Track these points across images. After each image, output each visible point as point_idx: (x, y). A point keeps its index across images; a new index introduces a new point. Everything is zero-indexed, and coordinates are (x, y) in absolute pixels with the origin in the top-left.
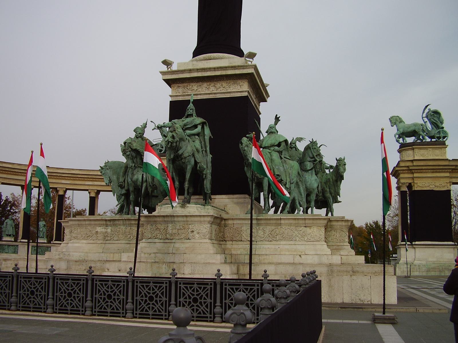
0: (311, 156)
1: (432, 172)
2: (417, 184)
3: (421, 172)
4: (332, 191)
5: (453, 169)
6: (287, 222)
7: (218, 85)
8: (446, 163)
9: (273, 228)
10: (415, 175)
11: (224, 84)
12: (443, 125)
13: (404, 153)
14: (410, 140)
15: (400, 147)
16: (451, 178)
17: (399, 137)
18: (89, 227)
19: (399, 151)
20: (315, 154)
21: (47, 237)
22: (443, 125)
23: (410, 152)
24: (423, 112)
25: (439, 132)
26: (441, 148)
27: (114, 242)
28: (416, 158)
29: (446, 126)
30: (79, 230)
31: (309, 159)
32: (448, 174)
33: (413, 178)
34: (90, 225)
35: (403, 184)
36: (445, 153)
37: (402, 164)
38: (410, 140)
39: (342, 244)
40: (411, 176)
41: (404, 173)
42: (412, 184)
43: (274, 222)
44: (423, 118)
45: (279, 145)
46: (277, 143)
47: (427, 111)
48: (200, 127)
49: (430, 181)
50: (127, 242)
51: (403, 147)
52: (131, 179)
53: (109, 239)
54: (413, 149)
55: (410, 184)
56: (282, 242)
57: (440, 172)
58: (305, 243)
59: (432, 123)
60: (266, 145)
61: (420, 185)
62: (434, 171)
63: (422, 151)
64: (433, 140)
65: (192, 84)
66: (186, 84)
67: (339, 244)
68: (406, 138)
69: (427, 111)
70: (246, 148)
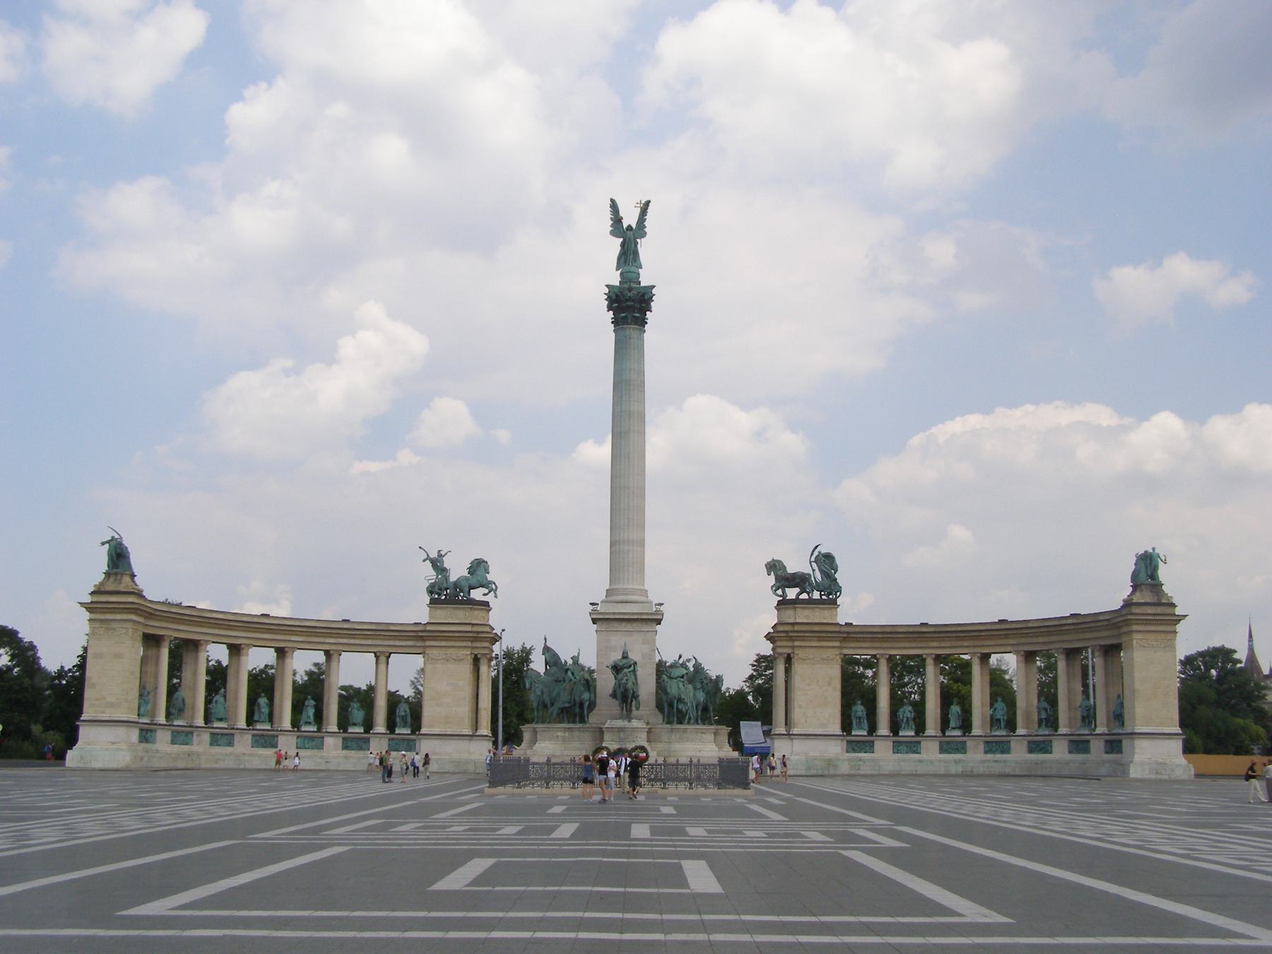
8: (837, 629)
10: (797, 643)
14: (792, 593)
15: (779, 603)
32: (837, 644)
33: (793, 647)
35: (780, 654)
37: (780, 628)
38: (792, 593)
40: (790, 644)
47: (816, 553)
51: (783, 604)
59: (821, 571)
62: (820, 639)
63: (807, 612)
69: (816, 553)
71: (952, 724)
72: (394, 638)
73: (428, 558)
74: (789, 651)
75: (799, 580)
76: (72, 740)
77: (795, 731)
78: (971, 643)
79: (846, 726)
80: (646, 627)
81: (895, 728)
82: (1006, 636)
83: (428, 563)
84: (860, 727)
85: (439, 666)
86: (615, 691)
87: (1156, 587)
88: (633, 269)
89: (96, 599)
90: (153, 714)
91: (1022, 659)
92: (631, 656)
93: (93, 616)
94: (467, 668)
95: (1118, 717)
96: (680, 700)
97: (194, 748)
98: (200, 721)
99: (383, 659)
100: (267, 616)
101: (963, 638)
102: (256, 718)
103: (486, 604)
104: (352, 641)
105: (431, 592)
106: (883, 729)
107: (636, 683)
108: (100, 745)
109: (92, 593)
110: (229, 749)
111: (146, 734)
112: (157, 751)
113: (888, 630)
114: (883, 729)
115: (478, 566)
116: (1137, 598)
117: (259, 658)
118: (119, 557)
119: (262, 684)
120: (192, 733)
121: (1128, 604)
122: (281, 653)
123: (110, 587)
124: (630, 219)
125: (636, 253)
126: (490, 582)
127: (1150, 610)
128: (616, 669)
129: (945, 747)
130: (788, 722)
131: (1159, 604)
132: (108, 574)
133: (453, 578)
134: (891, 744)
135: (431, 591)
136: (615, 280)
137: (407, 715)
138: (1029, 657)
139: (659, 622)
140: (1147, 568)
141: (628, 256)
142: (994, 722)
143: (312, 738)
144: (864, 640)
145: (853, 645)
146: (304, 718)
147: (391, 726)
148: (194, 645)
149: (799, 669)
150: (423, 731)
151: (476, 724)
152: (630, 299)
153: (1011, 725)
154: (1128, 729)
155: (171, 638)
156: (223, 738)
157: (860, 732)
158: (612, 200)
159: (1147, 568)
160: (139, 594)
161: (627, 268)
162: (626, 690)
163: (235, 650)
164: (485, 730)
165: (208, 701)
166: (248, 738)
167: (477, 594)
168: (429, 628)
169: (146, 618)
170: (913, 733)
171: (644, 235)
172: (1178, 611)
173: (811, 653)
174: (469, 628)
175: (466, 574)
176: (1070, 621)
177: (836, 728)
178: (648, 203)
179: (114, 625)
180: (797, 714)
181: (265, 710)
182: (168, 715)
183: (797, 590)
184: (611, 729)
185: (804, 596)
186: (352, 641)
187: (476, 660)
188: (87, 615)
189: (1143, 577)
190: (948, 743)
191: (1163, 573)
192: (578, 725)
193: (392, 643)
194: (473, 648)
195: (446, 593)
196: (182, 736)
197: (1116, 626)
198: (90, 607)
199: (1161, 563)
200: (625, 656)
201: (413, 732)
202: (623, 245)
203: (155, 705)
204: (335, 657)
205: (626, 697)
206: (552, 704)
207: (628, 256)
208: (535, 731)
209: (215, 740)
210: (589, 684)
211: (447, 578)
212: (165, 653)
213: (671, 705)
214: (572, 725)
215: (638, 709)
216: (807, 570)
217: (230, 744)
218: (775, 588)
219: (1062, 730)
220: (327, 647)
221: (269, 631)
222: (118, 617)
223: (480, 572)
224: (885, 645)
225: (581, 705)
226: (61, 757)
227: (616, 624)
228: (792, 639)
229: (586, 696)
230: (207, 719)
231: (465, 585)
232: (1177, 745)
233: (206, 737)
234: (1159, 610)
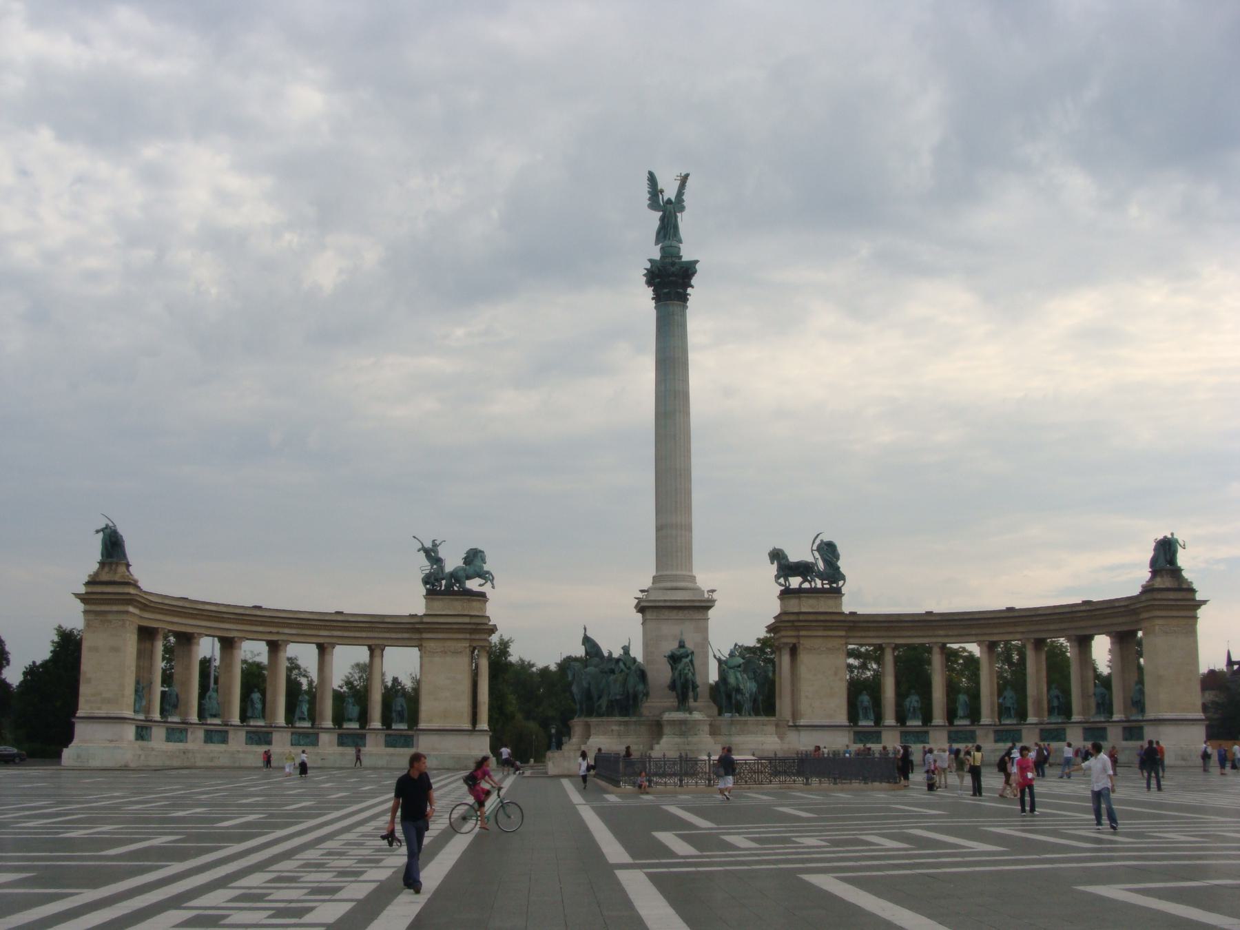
10: (803, 633)
14: (795, 582)
16: (847, 637)
28: (804, 610)
29: (843, 564)
32: (843, 633)
35: (786, 644)
37: (786, 618)
38: (795, 582)
40: (793, 633)
47: (818, 542)
51: (786, 593)
59: (824, 560)
62: (826, 628)
63: (811, 602)
71: (960, 712)
72: (389, 630)
75: (803, 569)
76: (67, 737)
77: (802, 722)
78: (978, 631)
79: (853, 716)
80: (697, 615)
81: (901, 718)
82: (1015, 624)
83: (422, 554)
84: (866, 717)
87: (1176, 572)
88: (675, 243)
89: (90, 590)
90: (147, 710)
91: (985, 649)
92: (687, 645)
93: (88, 608)
95: (1138, 704)
96: (738, 690)
97: (190, 746)
98: (194, 718)
100: (259, 608)
102: (249, 714)
103: (482, 596)
104: (346, 634)
106: (890, 720)
108: (91, 744)
109: (88, 584)
110: (222, 747)
111: (142, 733)
112: (153, 749)
114: (890, 720)
115: (474, 557)
116: (1159, 583)
117: (254, 650)
118: (113, 546)
119: (254, 679)
120: (186, 730)
121: (1147, 589)
122: (274, 647)
123: (105, 577)
124: (670, 193)
125: (676, 227)
126: (488, 572)
127: (1172, 595)
128: (674, 659)
130: (795, 714)
131: (1180, 589)
132: (102, 564)
133: (449, 567)
135: (426, 581)
136: (656, 254)
137: (402, 707)
138: (991, 647)
139: (709, 608)
140: (1166, 551)
141: (668, 230)
142: (1003, 711)
143: (306, 735)
144: (868, 629)
145: (859, 634)
146: (298, 714)
147: (387, 721)
148: (186, 640)
149: (805, 659)
150: (422, 726)
151: (474, 719)
152: (673, 274)
153: (1022, 715)
154: (1150, 715)
155: (168, 629)
156: (217, 736)
157: (866, 723)
158: (651, 174)
159: (1166, 551)
160: (135, 584)
161: (667, 243)
162: (687, 681)
163: (228, 644)
164: (484, 725)
165: (202, 696)
166: (242, 735)
167: (473, 584)
168: (426, 620)
169: (141, 609)
171: (682, 209)
172: (1199, 597)
174: (467, 620)
175: (460, 563)
176: (1083, 608)
177: (842, 719)
178: (687, 176)
179: (110, 617)
180: (804, 706)
181: (259, 706)
182: (163, 712)
183: (799, 579)
184: (672, 723)
185: (806, 585)
186: (346, 634)
188: (80, 606)
189: (1162, 562)
190: (957, 732)
191: (1183, 559)
192: (634, 719)
193: (387, 635)
195: (442, 584)
196: (176, 733)
197: (1135, 612)
198: (84, 599)
199: (1180, 550)
200: (682, 645)
201: (410, 728)
202: (662, 219)
203: (150, 702)
205: (683, 689)
206: (600, 697)
207: (668, 230)
208: (588, 727)
209: (210, 737)
210: (642, 675)
211: (442, 568)
212: (159, 647)
213: (729, 697)
214: (626, 719)
215: (695, 700)
216: (810, 559)
217: (224, 741)
218: (777, 577)
219: (1075, 718)
220: (321, 640)
221: (262, 624)
222: (115, 608)
223: (478, 562)
224: (892, 634)
225: (635, 697)
226: (58, 756)
227: (666, 614)
228: (797, 629)
229: (640, 687)
230: (201, 714)
231: (461, 574)
232: (1199, 732)
233: (200, 734)
234: (1180, 595)
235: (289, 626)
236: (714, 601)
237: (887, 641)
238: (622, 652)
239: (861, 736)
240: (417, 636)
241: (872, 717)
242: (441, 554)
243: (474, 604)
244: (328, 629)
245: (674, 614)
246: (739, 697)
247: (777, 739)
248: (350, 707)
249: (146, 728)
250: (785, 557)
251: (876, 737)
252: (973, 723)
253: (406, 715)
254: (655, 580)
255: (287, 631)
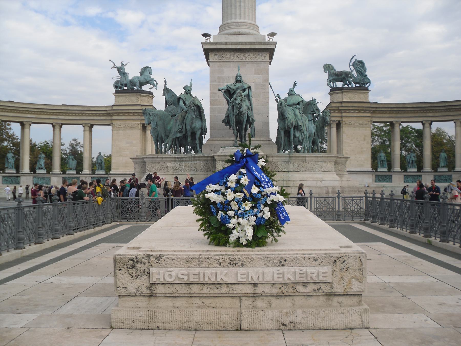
0: (312, 110)
1: (357, 112)
2: (345, 121)
3: (348, 112)
4: (319, 134)
5: (374, 110)
6: (310, 158)
7: (247, 55)
8: (369, 105)
9: (300, 162)
10: (344, 114)
11: (252, 55)
12: (366, 73)
13: (334, 96)
14: (339, 84)
15: (331, 90)
16: (372, 117)
17: (330, 81)
18: (161, 163)
19: (330, 94)
20: (315, 109)
21: (46, 168)
22: (366, 73)
23: (340, 95)
24: (350, 61)
25: (363, 79)
26: (365, 93)
27: (181, 173)
30: (152, 165)
31: (310, 112)
32: (369, 115)
33: (341, 117)
34: (161, 161)
35: (334, 121)
36: (368, 97)
37: (333, 105)
38: (339, 84)
39: (342, 173)
40: (339, 115)
41: (335, 112)
42: (341, 121)
43: (301, 158)
44: (350, 66)
45: (298, 104)
46: (297, 103)
47: (353, 60)
48: (247, 90)
49: (355, 119)
50: (192, 173)
51: (334, 90)
52: (191, 127)
53: (178, 171)
54: (342, 93)
55: (339, 121)
56: (306, 173)
57: (363, 113)
58: (322, 173)
59: (357, 71)
60: (290, 104)
61: (347, 123)
62: (359, 111)
63: (350, 95)
64: (357, 85)
65: (226, 53)
66: (221, 53)
67: (340, 173)
68: (337, 83)
70: (284, 108)
71: (442, 164)
72: (94, 115)
73: (114, 66)
74: (339, 119)
79: (375, 167)
83: (115, 69)
84: (383, 166)
85: (121, 132)
86: (228, 117)
94: (138, 132)
96: (297, 127)
99: (87, 128)
101: (450, 110)
103: (151, 93)
105: (116, 87)
107: (250, 108)
113: (401, 106)
126: (152, 80)
129: (437, 178)
134: (402, 177)
144: (385, 112)
149: (345, 129)
150: (112, 172)
157: (383, 170)
162: (240, 113)
167: (145, 88)
168: (114, 108)
170: (416, 170)
173: (353, 120)
174: (139, 108)
175: (139, 75)
177: (368, 167)
187: (144, 128)
190: (440, 176)
193: (92, 118)
194: (142, 120)
200: (238, 80)
204: (57, 127)
210: (199, 110)
221: (12, 111)
223: (147, 73)
224: (399, 115)
225: (193, 134)
227: (228, 55)
228: (340, 111)
235: (30, 112)
236: (275, 43)
237: (397, 120)
238: (183, 92)
239: (380, 178)
240: (109, 118)
241: (386, 166)
242: (126, 71)
243: (144, 98)
244: (58, 115)
245: (236, 57)
246: (298, 134)
247: (335, 176)
248: (71, 161)
249: (17, 177)
250: (333, 69)
251: (387, 178)
252: (449, 171)
253: (104, 166)
254: (221, 28)
255: (29, 116)
